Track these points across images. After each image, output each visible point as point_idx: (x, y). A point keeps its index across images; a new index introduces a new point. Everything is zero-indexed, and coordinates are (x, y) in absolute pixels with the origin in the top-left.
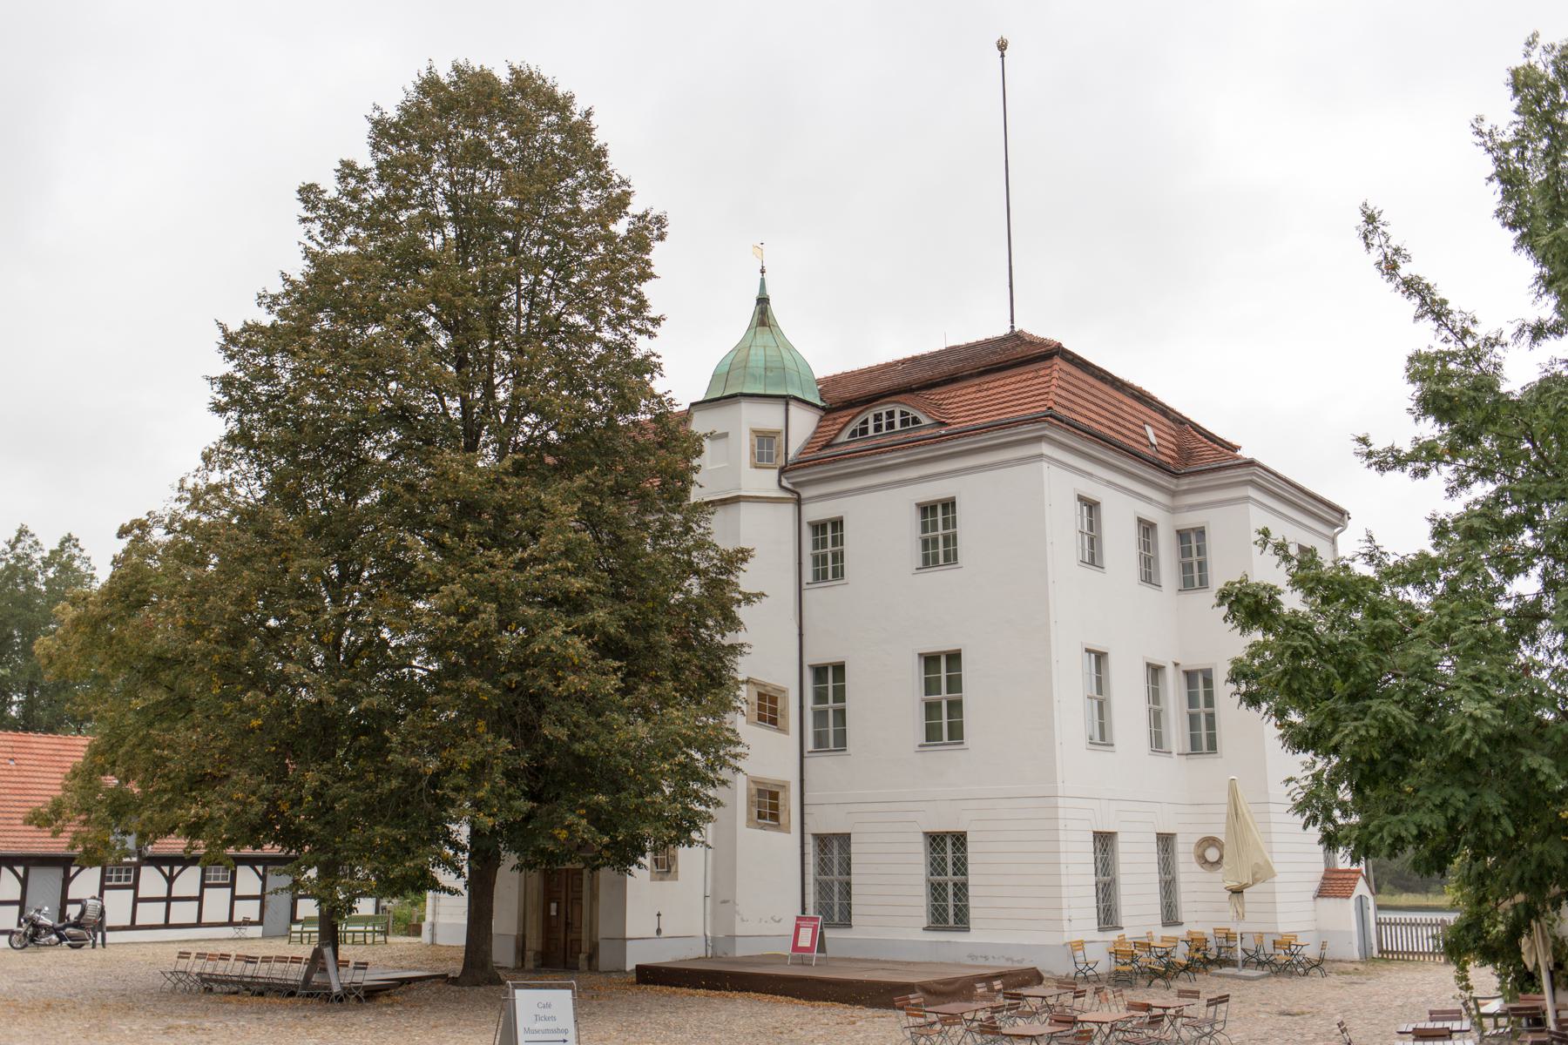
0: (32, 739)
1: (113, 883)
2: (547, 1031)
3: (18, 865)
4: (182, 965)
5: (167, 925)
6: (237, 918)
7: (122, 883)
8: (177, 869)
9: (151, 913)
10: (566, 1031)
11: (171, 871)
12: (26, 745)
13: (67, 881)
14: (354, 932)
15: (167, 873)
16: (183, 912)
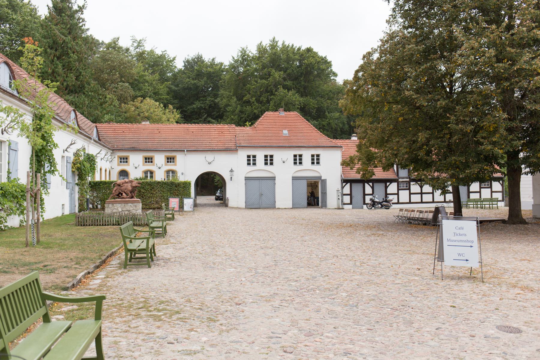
1: (402, 188)
2: (461, 241)
3: (370, 182)
4: (401, 214)
5: (422, 202)
6: (447, 200)
7: (405, 188)
9: (416, 198)
10: (472, 242)
11: (421, 184)
13: (386, 187)
14: (485, 204)
16: (427, 198)
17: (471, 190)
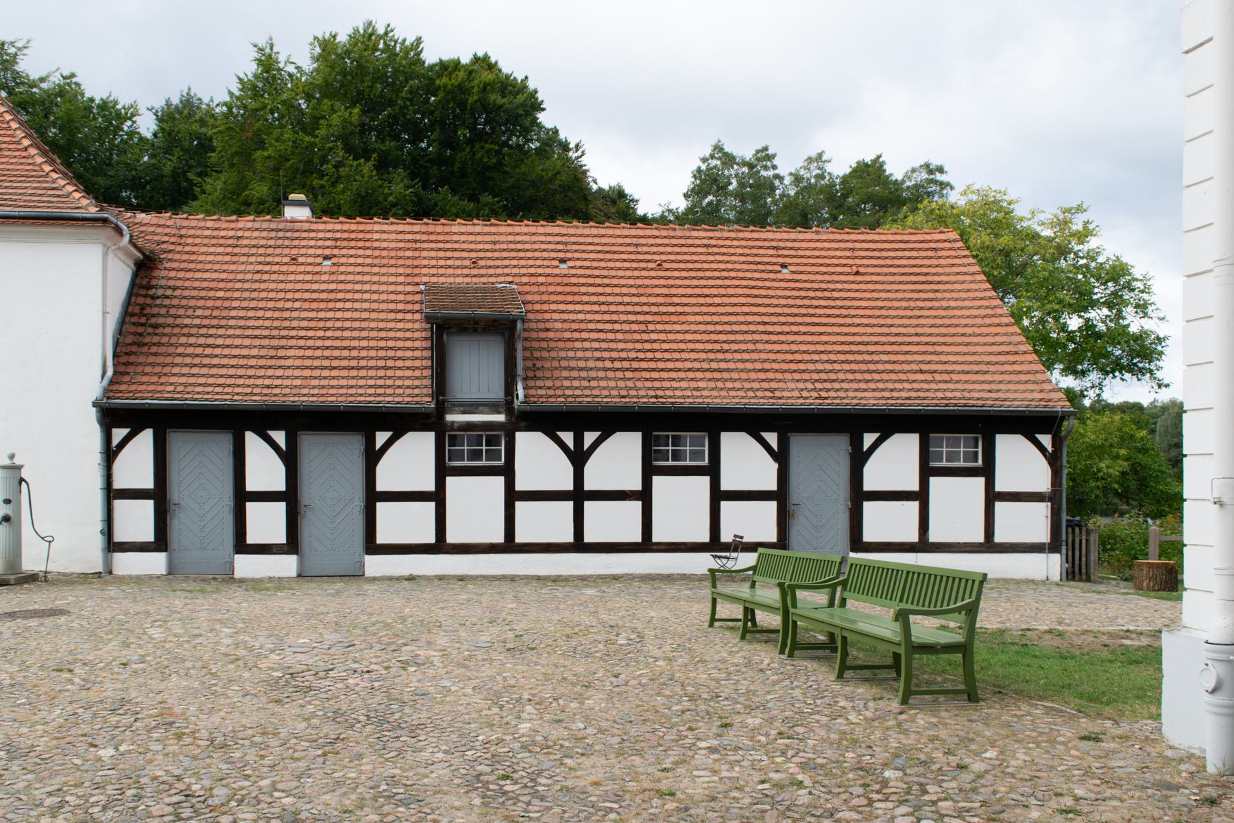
0: (376, 227)
5: (579, 545)
8: (590, 438)
11: (579, 440)
12: (361, 236)
15: (571, 446)
17: (875, 476)
